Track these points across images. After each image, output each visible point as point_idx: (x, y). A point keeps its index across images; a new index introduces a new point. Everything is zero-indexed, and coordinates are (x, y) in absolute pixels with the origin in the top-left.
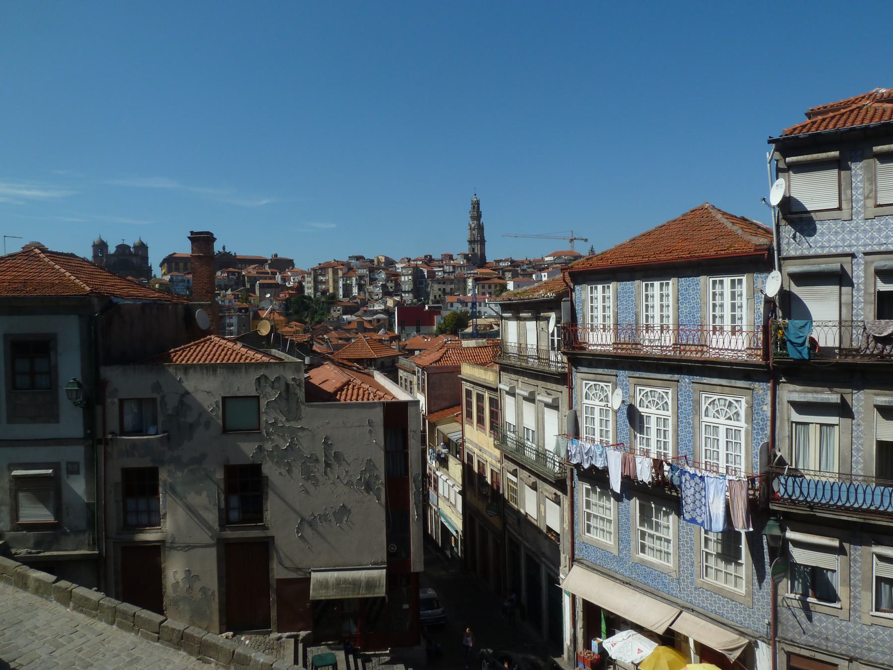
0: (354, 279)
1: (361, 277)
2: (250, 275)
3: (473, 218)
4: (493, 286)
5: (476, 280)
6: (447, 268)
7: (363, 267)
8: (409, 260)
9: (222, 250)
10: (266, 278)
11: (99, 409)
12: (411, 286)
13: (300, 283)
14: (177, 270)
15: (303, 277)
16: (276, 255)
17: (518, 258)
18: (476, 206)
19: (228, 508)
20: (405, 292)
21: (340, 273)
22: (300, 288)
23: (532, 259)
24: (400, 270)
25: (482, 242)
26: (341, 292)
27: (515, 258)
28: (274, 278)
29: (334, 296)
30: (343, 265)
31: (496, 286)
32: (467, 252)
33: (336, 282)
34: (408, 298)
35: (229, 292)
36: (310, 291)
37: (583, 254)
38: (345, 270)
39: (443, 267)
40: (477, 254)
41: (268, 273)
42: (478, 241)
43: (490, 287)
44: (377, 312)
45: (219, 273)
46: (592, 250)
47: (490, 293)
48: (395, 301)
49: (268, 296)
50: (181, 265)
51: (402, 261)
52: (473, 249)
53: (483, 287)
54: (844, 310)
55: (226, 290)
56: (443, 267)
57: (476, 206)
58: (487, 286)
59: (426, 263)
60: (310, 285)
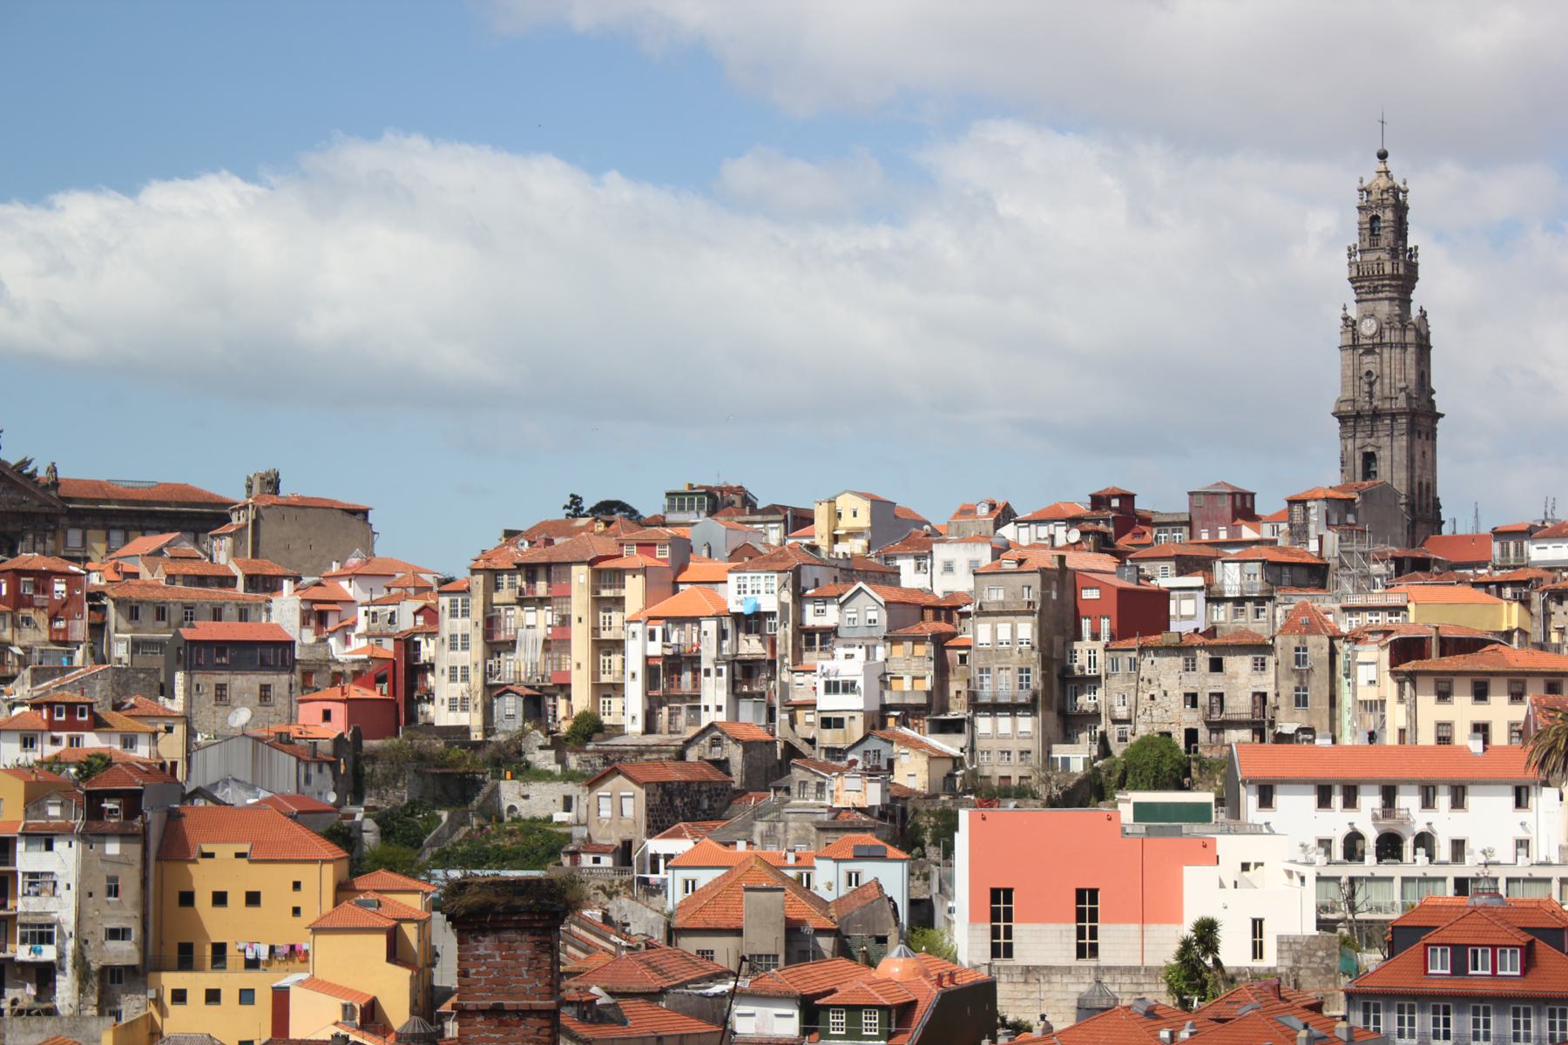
0: (710, 626)
1: (751, 622)
2: (133, 592)
3: (1364, 282)
5: (1405, 650)
6: (1231, 577)
7: (745, 556)
8: (1005, 515)
10: (217, 615)
12: (1036, 681)
15: (430, 613)
16: (272, 483)
20: (995, 708)
21: (634, 589)
24: (961, 582)
25: (1421, 418)
31: (1517, 697)
33: (607, 647)
40: (1387, 488)
41: (227, 581)
42: (1393, 416)
44: (837, 823)
47: (1482, 729)
48: (935, 757)
49: (241, 717)
52: (1369, 458)
59: (1104, 544)
60: (463, 658)
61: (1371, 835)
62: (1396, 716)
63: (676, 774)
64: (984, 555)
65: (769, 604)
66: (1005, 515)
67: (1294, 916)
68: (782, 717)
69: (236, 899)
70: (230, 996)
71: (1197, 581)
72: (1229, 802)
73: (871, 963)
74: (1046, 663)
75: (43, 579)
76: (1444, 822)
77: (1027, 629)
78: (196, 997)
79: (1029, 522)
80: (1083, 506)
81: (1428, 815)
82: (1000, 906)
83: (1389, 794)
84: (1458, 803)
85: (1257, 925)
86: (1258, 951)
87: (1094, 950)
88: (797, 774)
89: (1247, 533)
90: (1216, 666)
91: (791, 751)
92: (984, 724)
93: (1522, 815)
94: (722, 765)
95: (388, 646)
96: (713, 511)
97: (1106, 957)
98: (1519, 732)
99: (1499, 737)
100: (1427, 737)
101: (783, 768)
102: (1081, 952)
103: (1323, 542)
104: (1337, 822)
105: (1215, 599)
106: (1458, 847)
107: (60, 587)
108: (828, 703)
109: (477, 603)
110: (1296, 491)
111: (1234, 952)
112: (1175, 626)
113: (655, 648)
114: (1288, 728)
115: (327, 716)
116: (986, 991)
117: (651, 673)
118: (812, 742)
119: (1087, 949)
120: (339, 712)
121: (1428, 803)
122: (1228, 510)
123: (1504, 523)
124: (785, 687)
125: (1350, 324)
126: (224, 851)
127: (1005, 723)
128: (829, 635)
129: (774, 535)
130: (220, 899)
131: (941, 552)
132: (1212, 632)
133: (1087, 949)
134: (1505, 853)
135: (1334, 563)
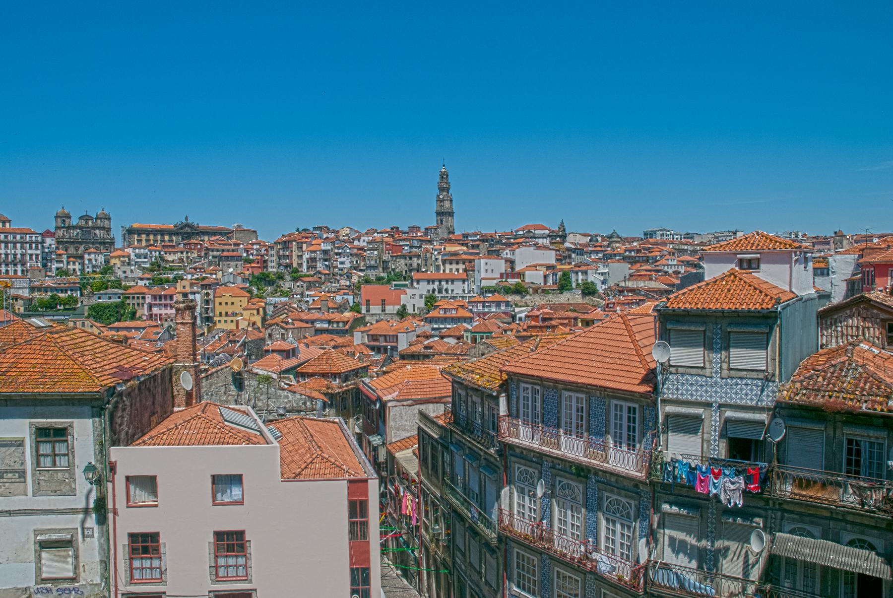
1: (325, 252)
3: (441, 189)
8: (376, 231)
9: (184, 221)
11: (110, 485)
13: (262, 256)
17: (488, 231)
18: (444, 176)
19: (217, 567)
21: (304, 246)
23: (500, 231)
25: (451, 214)
26: (305, 265)
27: (483, 232)
29: (296, 271)
31: (464, 263)
32: (434, 224)
37: (553, 229)
46: (562, 224)
48: (360, 277)
49: (231, 270)
51: (367, 234)
52: (442, 221)
54: (705, 446)
57: (444, 176)
62: (442, 268)
63: (311, 279)
65: (329, 248)
66: (376, 231)
67: (421, 303)
69: (230, 304)
70: (229, 321)
72: (412, 284)
74: (380, 258)
76: (450, 286)
78: (223, 321)
80: (389, 230)
83: (440, 281)
84: (452, 283)
85: (414, 305)
90: (411, 258)
97: (387, 312)
98: (465, 270)
99: (461, 271)
100: (448, 271)
104: (431, 287)
105: (411, 247)
106: (452, 291)
108: (340, 266)
111: (410, 310)
113: (308, 256)
116: (364, 318)
117: (308, 262)
119: (383, 310)
121: (447, 283)
125: (438, 196)
126: (227, 295)
128: (340, 254)
130: (227, 304)
131: (363, 238)
133: (383, 310)
134: (460, 292)
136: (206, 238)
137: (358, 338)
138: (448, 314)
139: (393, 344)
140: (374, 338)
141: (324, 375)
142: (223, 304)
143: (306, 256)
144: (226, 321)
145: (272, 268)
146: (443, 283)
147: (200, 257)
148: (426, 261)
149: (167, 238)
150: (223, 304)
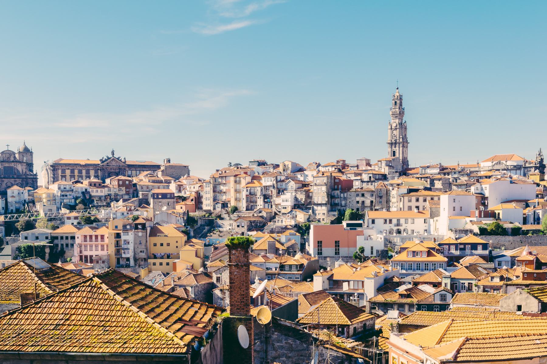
2: (141, 183)
4: (421, 199)
8: (319, 165)
9: (110, 156)
10: (159, 188)
13: (198, 193)
14: (64, 177)
16: (169, 161)
22: (198, 200)
28: (168, 187)
30: (246, 173)
34: (321, 212)
35: (121, 202)
36: (208, 202)
38: (249, 179)
39: (360, 175)
41: (161, 182)
43: (417, 200)
45: (108, 181)
47: (417, 207)
50: (68, 172)
53: (410, 201)
55: (117, 201)
56: (360, 175)
58: (414, 199)
59: (340, 171)
61: (395, 228)
64: (315, 173)
66: (319, 165)
68: (274, 206)
70: (164, 264)
71: (359, 178)
73: (294, 256)
75: (124, 181)
77: (324, 188)
79: (324, 166)
81: (406, 225)
82: (319, 244)
83: (398, 220)
85: (372, 248)
86: (372, 253)
87: (339, 253)
88: (277, 218)
89: (369, 168)
91: (276, 214)
92: (315, 207)
93: (426, 224)
94: (262, 217)
95: (194, 193)
96: (259, 165)
97: (341, 255)
101: (274, 217)
102: (336, 254)
103: (385, 170)
104: (388, 226)
107: (127, 182)
108: (284, 204)
109: (212, 185)
110: (380, 159)
112: (354, 187)
113: (248, 193)
114: (377, 208)
115: (181, 208)
118: (280, 212)
119: (337, 253)
120: (184, 207)
122: (365, 164)
123: (422, 166)
124: (274, 201)
127: (319, 208)
129: (272, 170)
130: (162, 245)
132: (362, 188)
133: (337, 253)
134: (422, 232)
135: (387, 174)
136: (134, 172)
137: (318, 283)
138: (418, 258)
139: (361, 291)
140: (337, 284)
141: (329, 327)
142: (158, 245)
143: (244, 194)
144: (161, 264)
145: (207, 204)
146: (402, 221)
147: (127, 193)
148: (381, 197)
149: (92, 173)
150: (158, 245)
